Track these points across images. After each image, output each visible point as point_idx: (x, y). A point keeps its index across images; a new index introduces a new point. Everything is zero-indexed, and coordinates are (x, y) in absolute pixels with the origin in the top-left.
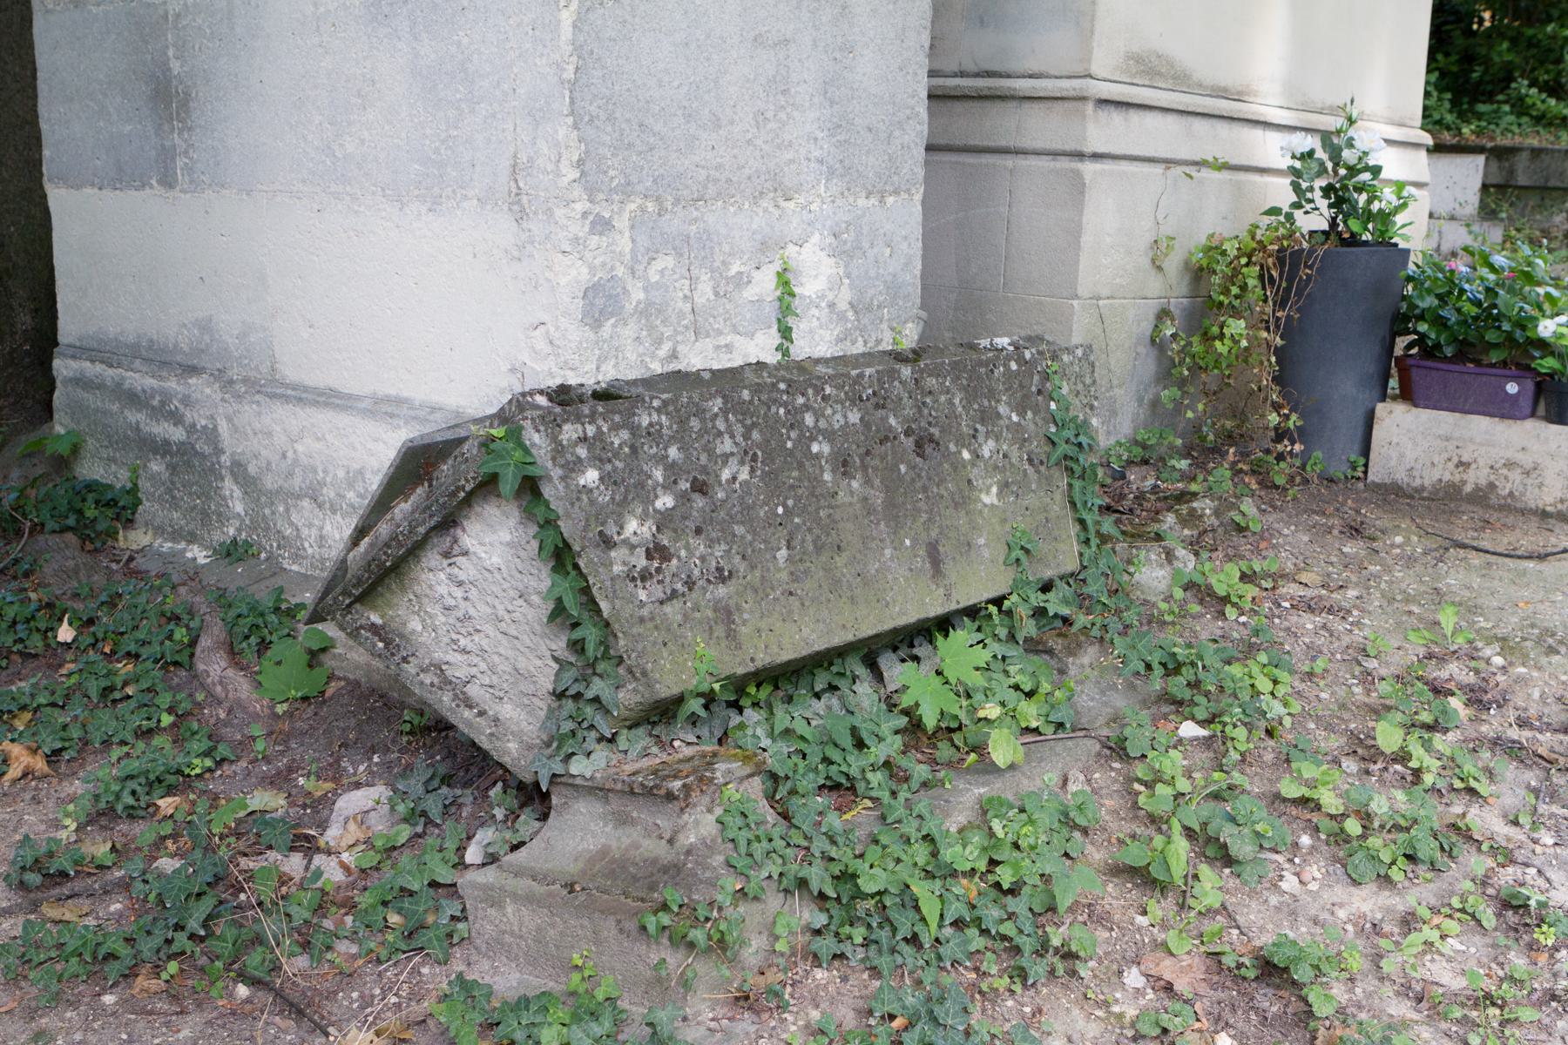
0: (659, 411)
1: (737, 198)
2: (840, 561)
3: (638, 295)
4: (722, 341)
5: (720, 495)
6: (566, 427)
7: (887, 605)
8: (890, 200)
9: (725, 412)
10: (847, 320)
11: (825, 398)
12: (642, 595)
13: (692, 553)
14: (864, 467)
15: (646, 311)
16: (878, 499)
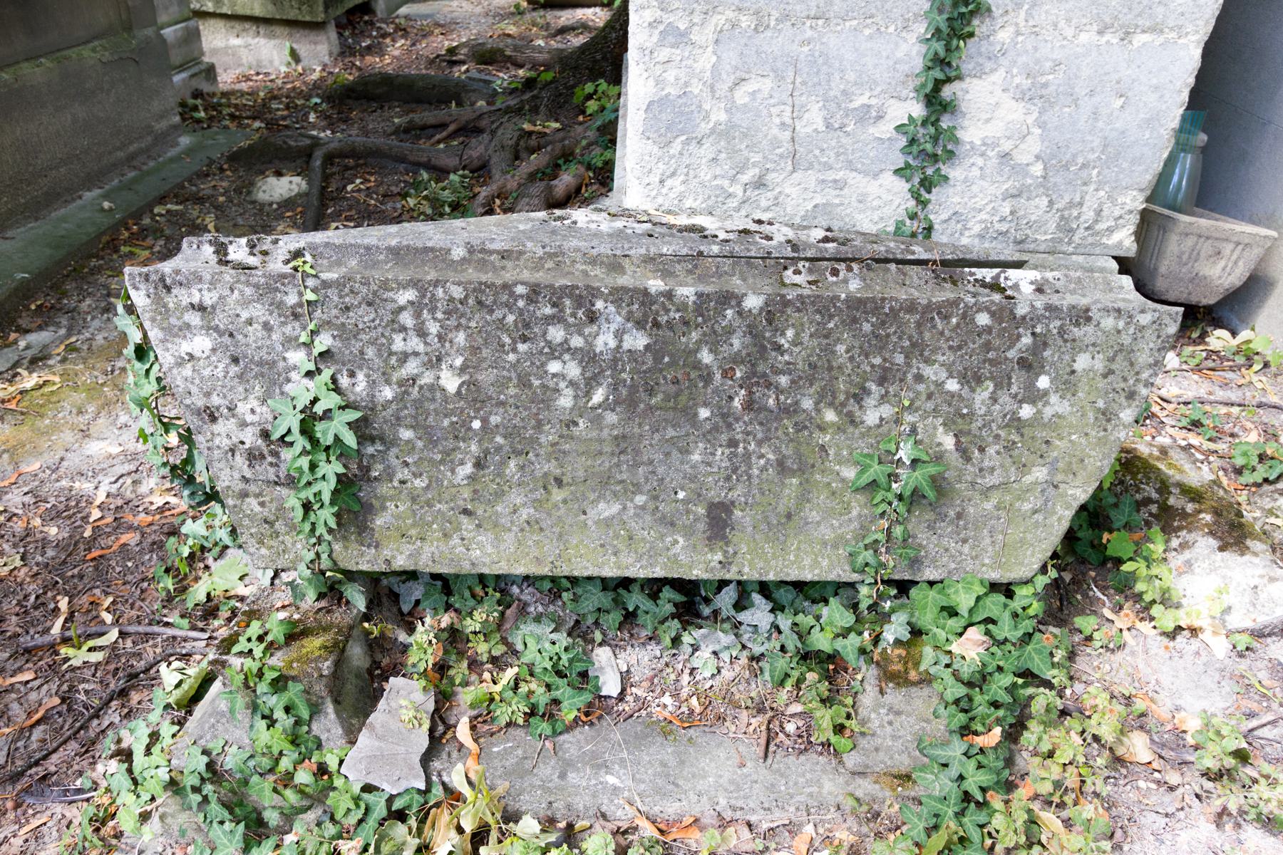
3: (719, 116)
4: (831, 175)
10: (1027, 174)
15: (724, 133)
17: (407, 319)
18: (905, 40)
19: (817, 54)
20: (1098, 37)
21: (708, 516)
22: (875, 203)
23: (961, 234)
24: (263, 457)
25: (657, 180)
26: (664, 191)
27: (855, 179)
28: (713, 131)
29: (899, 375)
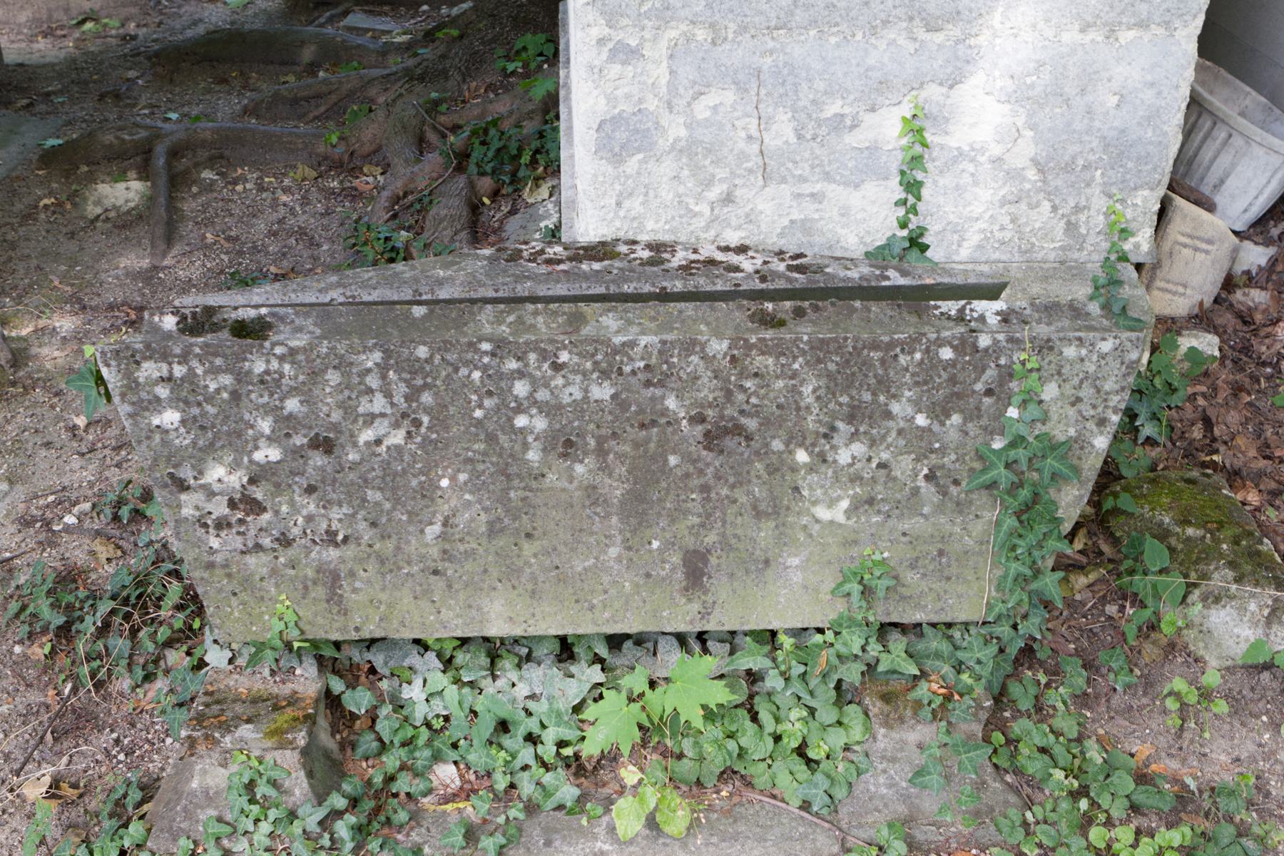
0: (282, 359)
1: (844, 27)
2: (528, 548)
3: (676, 130)
4: (807, 188)
5: (350, 457)
6: (145, 365)
7: (592, 608)
8: (1126, 36)
9: (383, 369)
10: (1024, 179)
11: (557, 367)
12: (215, 543)
13: (295, 511)
14: (601, 452)
15: (685, 150)
16: (616, 490)
17: (373, 381)
18: (876, 47)
19: (781, 64)
20: (1082, 36)
21: (684, 565)
22: (859, 217)
23: (959, 246)
24: (229, 525)
25: (613, 202)
26: (622, 213)
27: (833, 191)
28: (673, 147)
29: (868, 412)
